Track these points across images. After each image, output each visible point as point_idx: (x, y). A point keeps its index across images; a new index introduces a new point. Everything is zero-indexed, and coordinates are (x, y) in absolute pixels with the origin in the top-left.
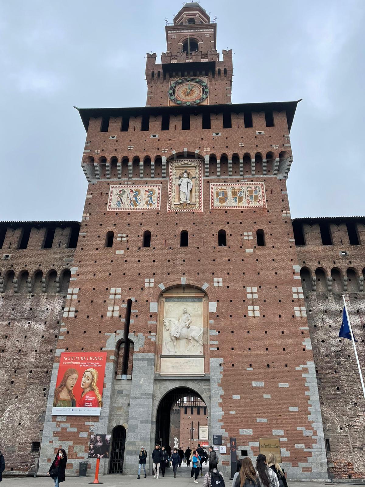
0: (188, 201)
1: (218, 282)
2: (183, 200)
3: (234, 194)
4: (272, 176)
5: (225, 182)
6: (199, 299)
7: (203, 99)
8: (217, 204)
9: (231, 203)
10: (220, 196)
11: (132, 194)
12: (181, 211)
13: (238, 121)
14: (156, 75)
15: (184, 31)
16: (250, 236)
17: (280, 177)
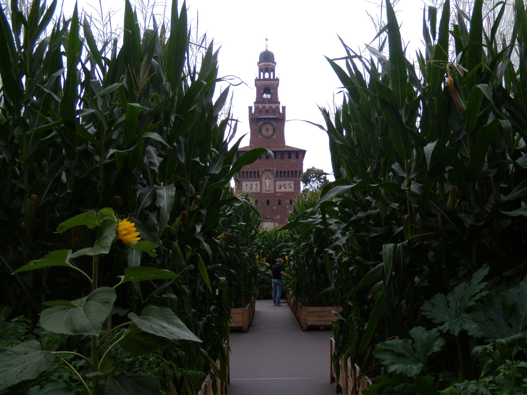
0: (269, 189)
1: (278, 217)
2: (267, 189)
3: (284, 186)
4: (296, 179)
5: (281, 181)
6: (273, 221)
7: (273, 135)
8: (278, 190)
9: (283, 190)
10: (279, 186)
11: (250, 185)
12: (266, 192)
13: (286, 156)
14: (253, 120)
15: (264, 82)
16: (288, 202)
17: (299, 179)
